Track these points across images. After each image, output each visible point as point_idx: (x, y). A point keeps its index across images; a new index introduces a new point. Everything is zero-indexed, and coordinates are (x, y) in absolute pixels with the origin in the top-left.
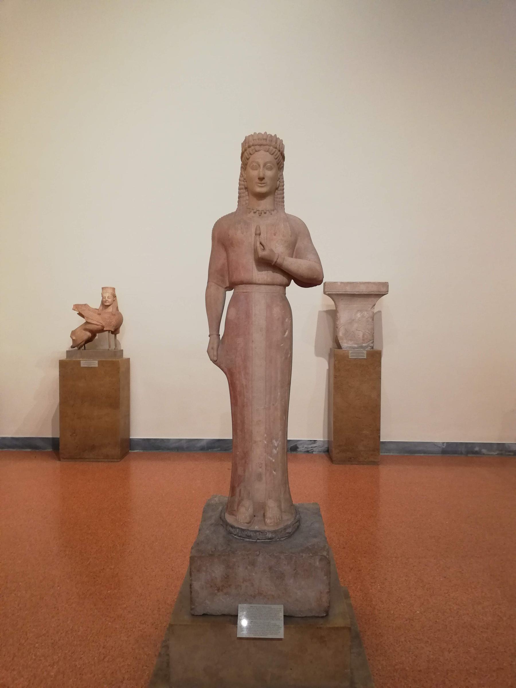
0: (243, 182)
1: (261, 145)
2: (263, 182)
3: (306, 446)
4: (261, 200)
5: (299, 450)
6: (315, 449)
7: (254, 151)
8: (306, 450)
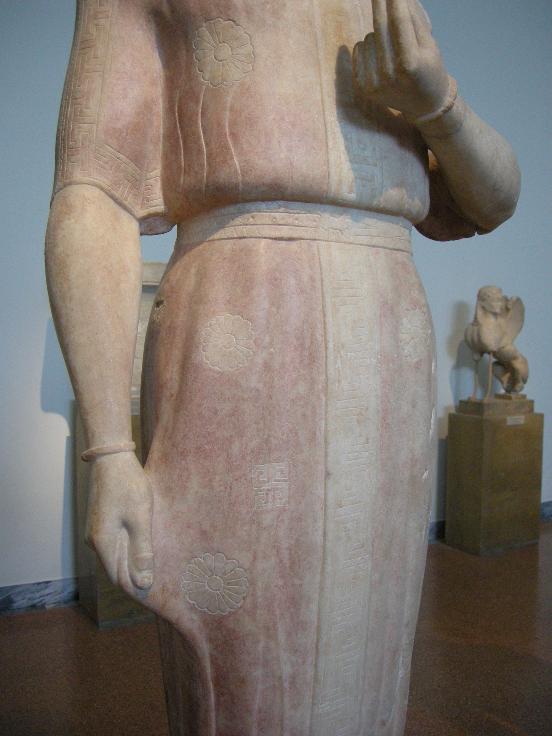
3: (28, 596)
5: (15, 605)
6: (47, 599)
8: (31, 603)
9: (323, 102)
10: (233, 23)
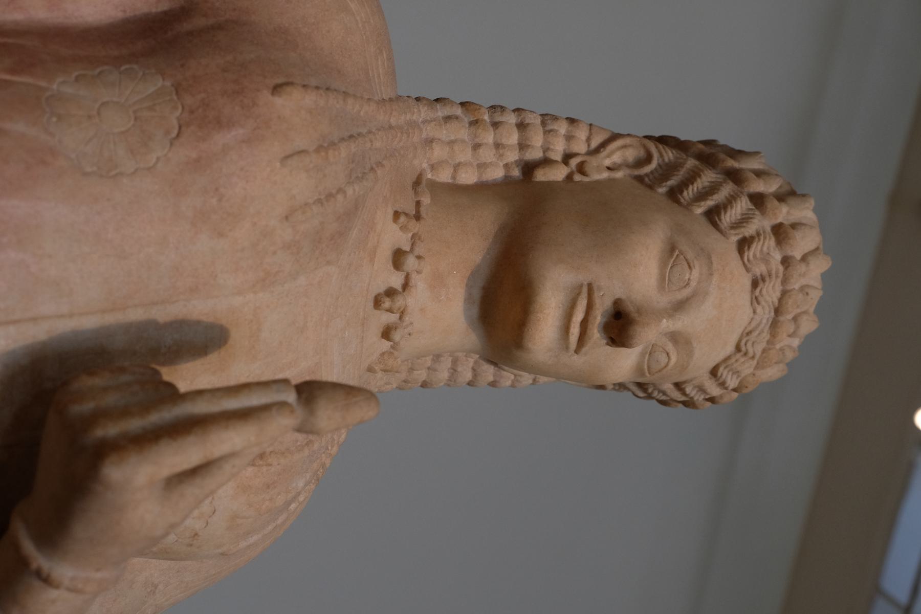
0: (558, 148)
1: (777, 311)
2: (596, 334)
4: (468, 300)
7: (760, 269)
9: (34, 320)
10: (174, 135)
